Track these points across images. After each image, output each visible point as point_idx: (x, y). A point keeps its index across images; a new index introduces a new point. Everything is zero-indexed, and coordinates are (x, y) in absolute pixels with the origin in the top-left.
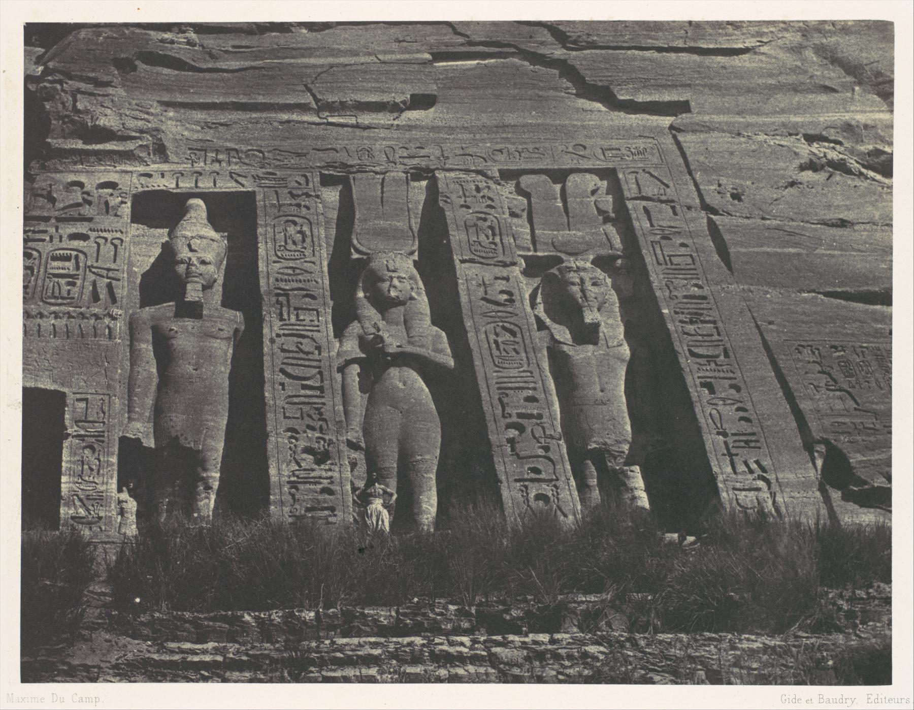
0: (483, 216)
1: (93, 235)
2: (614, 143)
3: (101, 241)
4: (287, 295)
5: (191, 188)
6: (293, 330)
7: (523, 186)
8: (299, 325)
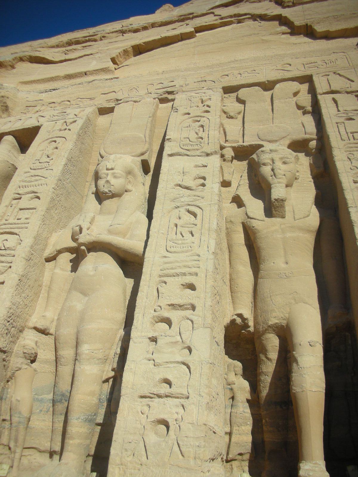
0: (198, 119)
2: (313, 59)
7: (240, 96)
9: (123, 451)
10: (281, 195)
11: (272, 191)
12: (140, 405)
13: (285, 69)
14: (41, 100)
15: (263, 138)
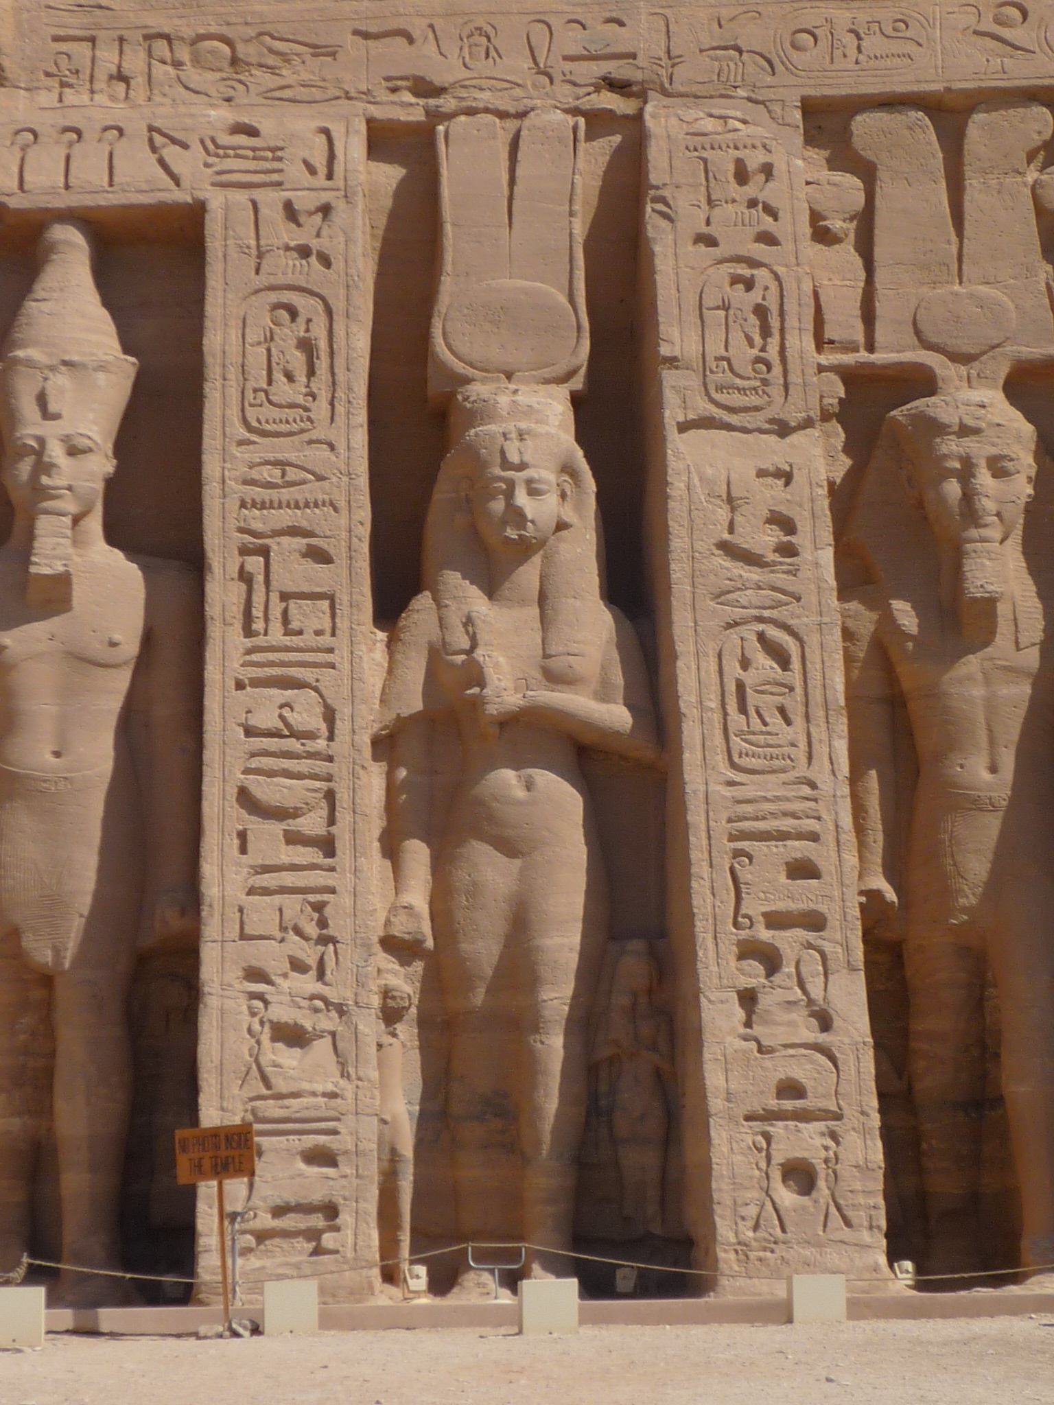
0: (745, 271)
4: (265, 552)
5: (52, 191)
6: (271, 664)
7: (858, 142)
8: (288, 649)
9: (739, 1221)
10: (990, 588)
11: (969, 565)
12: (748, 1134)
13: (1006, 33)
14: (100, 7)
15: (934, 339)
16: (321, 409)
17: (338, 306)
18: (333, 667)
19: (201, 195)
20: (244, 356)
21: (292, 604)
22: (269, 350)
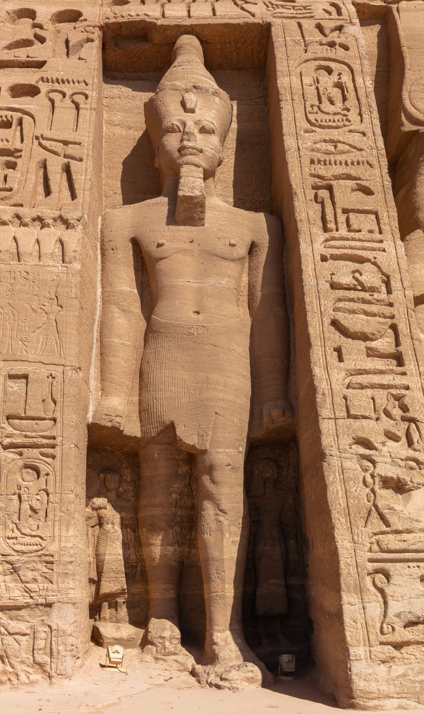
1: (44, 87)
3: (57, 97)
5: (182, 18)
8: (354, 239)
16: (353, 115)
17: (356, 67)
18: (384, 251)
19: (268, 20)
20: (303, 89)
21: (351, 215)
22: (317, 88)
